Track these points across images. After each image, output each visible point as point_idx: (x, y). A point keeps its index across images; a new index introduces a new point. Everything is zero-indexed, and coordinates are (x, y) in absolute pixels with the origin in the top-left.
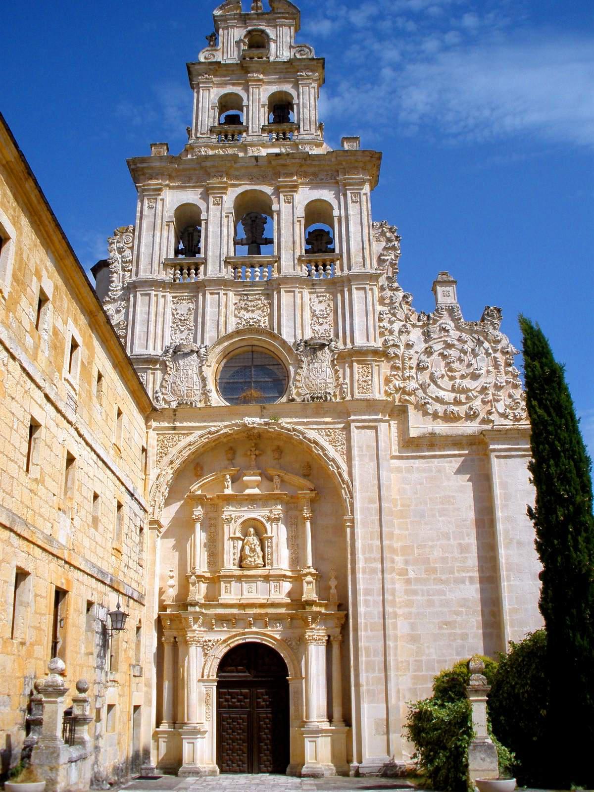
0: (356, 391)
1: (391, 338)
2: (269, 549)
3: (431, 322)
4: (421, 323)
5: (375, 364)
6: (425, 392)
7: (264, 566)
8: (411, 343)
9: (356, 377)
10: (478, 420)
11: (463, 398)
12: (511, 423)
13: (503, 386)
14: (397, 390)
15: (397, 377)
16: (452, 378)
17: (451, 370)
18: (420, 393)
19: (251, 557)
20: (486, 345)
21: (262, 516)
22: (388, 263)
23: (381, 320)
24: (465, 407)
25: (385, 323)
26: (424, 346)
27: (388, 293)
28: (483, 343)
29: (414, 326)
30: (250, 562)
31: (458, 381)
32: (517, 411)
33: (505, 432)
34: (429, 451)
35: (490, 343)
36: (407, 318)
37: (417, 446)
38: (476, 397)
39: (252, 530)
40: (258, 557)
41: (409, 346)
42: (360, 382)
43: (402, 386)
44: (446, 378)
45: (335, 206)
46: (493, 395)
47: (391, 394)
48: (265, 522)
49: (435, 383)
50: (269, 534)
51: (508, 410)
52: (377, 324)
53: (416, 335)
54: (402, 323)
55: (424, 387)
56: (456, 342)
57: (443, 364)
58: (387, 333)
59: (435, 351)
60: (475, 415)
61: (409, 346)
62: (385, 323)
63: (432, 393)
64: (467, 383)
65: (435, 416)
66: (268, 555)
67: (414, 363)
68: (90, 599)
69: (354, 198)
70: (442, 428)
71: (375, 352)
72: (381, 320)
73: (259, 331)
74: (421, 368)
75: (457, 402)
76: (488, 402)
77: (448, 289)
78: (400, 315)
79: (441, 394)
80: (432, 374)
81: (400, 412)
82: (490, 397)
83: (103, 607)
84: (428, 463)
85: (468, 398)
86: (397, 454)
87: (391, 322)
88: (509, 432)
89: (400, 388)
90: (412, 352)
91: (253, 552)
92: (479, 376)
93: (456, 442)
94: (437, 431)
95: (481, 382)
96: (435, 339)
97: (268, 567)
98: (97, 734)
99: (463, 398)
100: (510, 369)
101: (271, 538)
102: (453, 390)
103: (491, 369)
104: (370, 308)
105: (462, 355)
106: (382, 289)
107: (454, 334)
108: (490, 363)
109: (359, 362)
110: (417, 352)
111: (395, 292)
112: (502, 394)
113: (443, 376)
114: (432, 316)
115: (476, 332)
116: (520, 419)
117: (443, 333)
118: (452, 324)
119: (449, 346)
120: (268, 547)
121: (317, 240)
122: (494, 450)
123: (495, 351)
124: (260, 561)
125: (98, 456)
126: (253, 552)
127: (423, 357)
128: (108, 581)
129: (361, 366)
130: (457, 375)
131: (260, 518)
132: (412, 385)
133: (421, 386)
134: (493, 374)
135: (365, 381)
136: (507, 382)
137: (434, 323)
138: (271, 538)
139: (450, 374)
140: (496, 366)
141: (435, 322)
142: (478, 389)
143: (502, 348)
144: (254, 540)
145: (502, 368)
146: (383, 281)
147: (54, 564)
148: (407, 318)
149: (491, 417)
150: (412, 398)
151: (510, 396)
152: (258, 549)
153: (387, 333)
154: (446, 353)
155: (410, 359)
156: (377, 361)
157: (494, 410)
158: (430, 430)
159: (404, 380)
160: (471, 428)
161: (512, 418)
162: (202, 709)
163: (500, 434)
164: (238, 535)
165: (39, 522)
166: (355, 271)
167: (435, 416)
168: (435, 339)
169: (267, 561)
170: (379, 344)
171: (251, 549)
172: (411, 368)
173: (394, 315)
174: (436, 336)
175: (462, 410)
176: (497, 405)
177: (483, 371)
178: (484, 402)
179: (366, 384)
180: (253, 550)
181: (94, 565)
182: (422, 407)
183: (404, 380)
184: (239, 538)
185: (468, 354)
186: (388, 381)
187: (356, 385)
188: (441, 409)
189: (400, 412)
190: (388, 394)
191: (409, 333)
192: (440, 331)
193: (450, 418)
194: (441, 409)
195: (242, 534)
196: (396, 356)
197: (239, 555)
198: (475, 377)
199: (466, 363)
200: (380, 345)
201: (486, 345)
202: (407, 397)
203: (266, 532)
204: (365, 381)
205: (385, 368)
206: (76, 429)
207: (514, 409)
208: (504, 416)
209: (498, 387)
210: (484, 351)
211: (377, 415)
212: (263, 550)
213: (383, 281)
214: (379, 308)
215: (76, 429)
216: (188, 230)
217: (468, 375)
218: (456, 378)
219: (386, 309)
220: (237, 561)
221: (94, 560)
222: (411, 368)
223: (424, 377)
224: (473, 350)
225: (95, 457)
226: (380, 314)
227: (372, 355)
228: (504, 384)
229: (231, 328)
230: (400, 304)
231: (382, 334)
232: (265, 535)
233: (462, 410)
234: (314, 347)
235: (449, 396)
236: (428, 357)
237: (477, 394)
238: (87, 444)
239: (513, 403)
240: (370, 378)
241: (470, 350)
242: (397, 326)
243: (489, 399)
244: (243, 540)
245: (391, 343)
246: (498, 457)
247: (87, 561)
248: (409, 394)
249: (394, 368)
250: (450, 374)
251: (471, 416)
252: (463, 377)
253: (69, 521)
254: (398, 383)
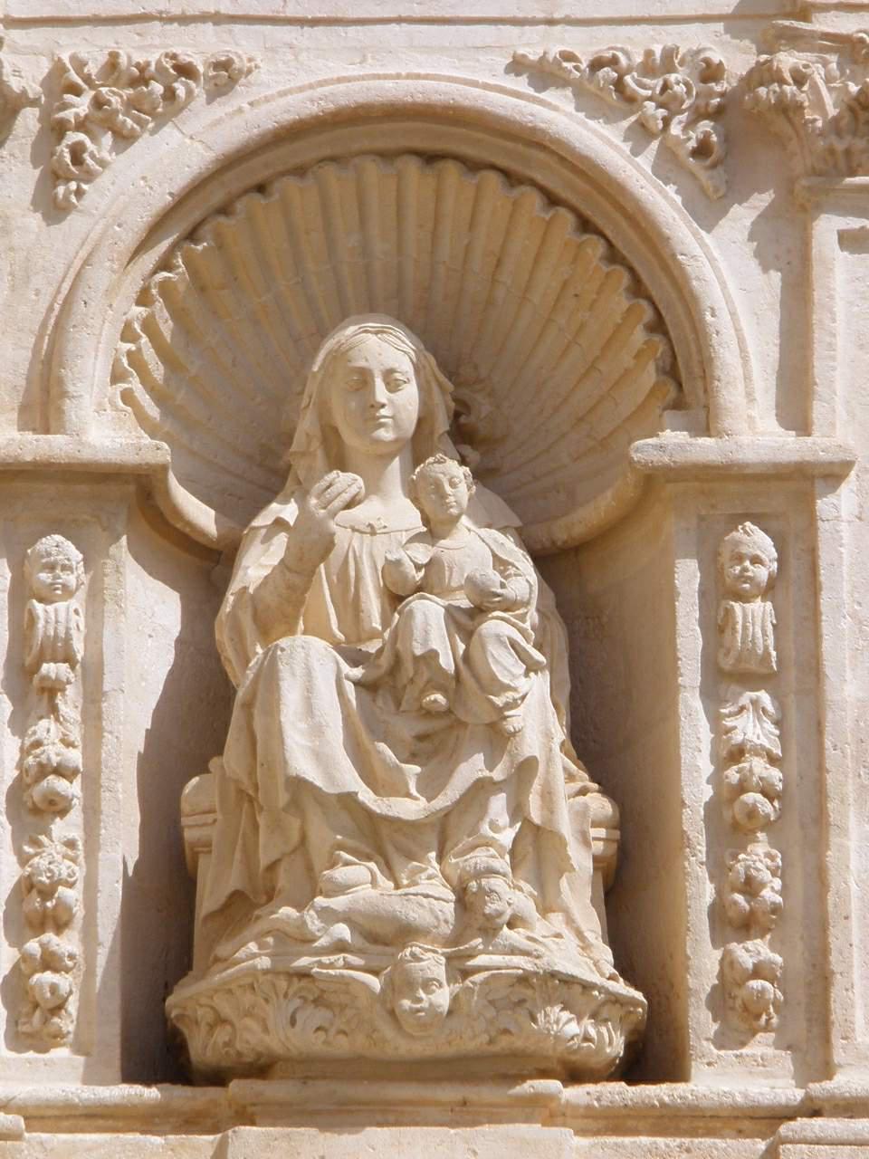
2: (753, 727)
7: (651, 1055)
19: (382, 841)
21: (607, 88)
30: (384, 937)
39: (386, 349)
40: (536, 849)
48: (664, 204)
50: (752, 431)
66: (731, 827)
91: (435, 743)
97: (719, 1075)
101: (790, 494)
120: (728, 675)
124: (572, 942)
126: (435, 743)
131: (559, 115)
138: (790, 494)
144: (405, 532)
152: (536, 715)
164: (104, 429)
169: (702, 962)
171: (386, 683)
180: (416, 707)
184: (133, 498)
195: (175, 408)
197: (123, 842)
203: (685, 383)
212: (610, 735)
220: (88, 955)
232: (672, 443)
244: (202, 568)
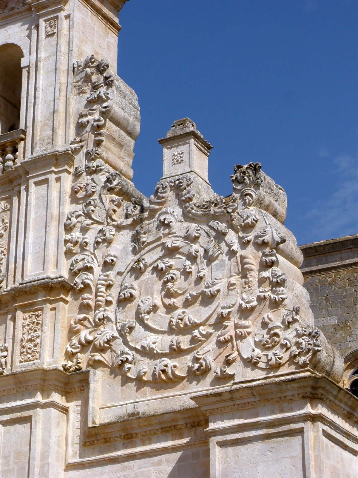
0: (17, 358)
3: (146, 214)
4: (130, 221)
5: (49, 306)
6: (126, 343)
8: (108, 259)
9: (19, 334)
10: (210, 377)
11: (184, 342)
12: (263, 374)
13: (253, 309)
14: (86, 345)
15: (86, 323)
16: (170, 309)
17: (169, 294)
18: (119, 345)
20: (232, 237)
22: (88, 128)
24: (189, 358)
25: (76, 234)
26: (132, 258)
27: (85, 179)
28: (225, 234)
29: (119, 228)
32: (274, 351)
33: (228, 396)
34: (125, 447)
35: (237, 232)
37: (106, 440)
38: (208, 336)
42: (24, 343)
43: (90, 338)
44: (162, 311)
45: (25, 51)
46: (236, 326)
47: (74, 354)
49: (141, 321)
51: (258, 351)
53: (122, 242)
54: (100, 227)
55: (125, 332)
56: (180, 243)
57: (159, 285)
58: (76, 249)
59: (146, 266)
60: (204, 372)
61: (108, 265)
62: (76, 234)
63: (137, 341)
64: (196, 314)
65: (140, 382)
69: (49, 29)
70: (151, 402)
72: (69, 229)
74: (124, 301)
75: (176, 352)
76: (226, 342)
77: (182, 149)
78: (99, 214)
79: (150, 340)
81: (73, 383)
82: (231, 332)
84: (124, 469)
85: (194, 340)
86: (77, 460)
87: (84, 230)
88: (236, 395)
89: (89, 342)
90: (112, 274)
92: (213, 297)
93: (167, 425)
94: (142, 408)
96: (149, 244)
99: (184, 342)
100: (266, 274)
102: (171, 330)
103: (236, 279)
105: (188, 263)
106: (77, 175)
107: (180, 227)
108: (234, 269)
109: (24, 309)
110: (120, 273)
111: (94, 176)
112: (252, 324)
113: (155, 308)
114: (146, 204)
115: (215, 217)
116: (279, 366)
117: (162, 231)
118: (178, 211)
119: (171, 252)
122: (215, 433)
123: (244, 244)
127: (129, 281)
129: (27, 315)
130: (178, 301)
132: (109, 331)
133: (119, 332)
134: (239, 289)
135: (31, 340)
136: (261, 300)
137: (151, 216)
139: (167, 301)
140: (244, 273)
141: (153, 212)
142: (212, 321)
143: (256, 237)
145: (254, 276)
149: (229, 371)
150: (106, 357)
151: (264, 325)
153: (76, 249)
154: (161, 265)
155: (109, 287)
156: (51, 302)
157: (235, 354)
158: (130, 409)
160: (182, 398)
161: (263, 365)
163: (224, 401)
166: (40, 153)
167: (140, 382)
168: (149, 244)
172: (108, 303)
173: (88, 215)
174: (151, 239)
175: (180, 366)
176: (242, 345)
177: (222, 285)
178: (221, 344)
179: (31, 345)
182: (118, 370)
185: (198, 261)
186: (72, 332)
187: (18, 349)
188: (146, 367)
189: (73, 383)
190: (70, 356)
191: (109, 242)
192: (158, 228)
193: (164, 381)
194: (146, 367)
196: (87, 287)
198: (208, 299)
199: (193, 277)
201: (232, 237)
202: (98, 357)
204: (31, 340)
205: (66, 311)
207: (269, 349)
208: (251, 363)
209: (245, 312)
210: (225, 249)
211: (32, 396)
213: (80, 161)
214: (68, 208)
217: (194, 298)
218: (176, 308)
219: (79, 208)
222: (108, 303)
223: (127, 316)
224: (206, 251)
227: (44, 293)
228: (255, 303)
230: (100, 195)
231: (69, 253)
233: (180, 366)
235: (160, 342)
236: (136, 278)
237: (211, 330)
239: (266, 337)
240: (39, 333)
241: (201, 252)
243: (227, 336)
245: (80, 265)
246: (222, 444)
248: (102, 350)
249: (85, 308)
250: (167, 301)
251: (198, 373)
252: (187, 304)
254: (85, 334)
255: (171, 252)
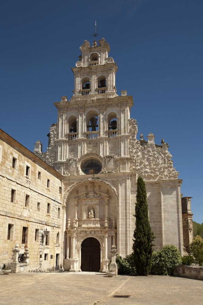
1: (132, 154)
23: (129, 149)
31: (152, 166)
36: (138, 148)
41: (138, 156)
52: (128, 150)
67: (139, 161)
68: (37, 228)
71: (127, 159)
72: (129, 149)
73: (93, 154)
80: (144, 164)
83: (42, 230)
87: (132, 150)
90: (139, 158)
95: (160, 166)
98: (40, 261)
104: (126, 145)
106: (131, 139)
121: (113, 124)
125: (39, 193)
128: (44, 223)
146: (131, 137)
147: (22, 222)
148: (138, 148)
159: (136, 166)
162: (77, 257)
165: (16, 213)
170: (128, 156)
181: (37, 220)
183: (136, 166)
200: (129, 156)
206: (30, 189)
213: (131, 137)
215: (30, 189)
216: (73, 127)
221: (38, 219)
222: (138, 163)
225: (38, 194)
226: (129, 147)
229: (85, 153)
234: (110, 157)
238: (34, 191)
242: (134, 151)
247: (35, 219)
253: (28, 211)
255: (151, 156)
